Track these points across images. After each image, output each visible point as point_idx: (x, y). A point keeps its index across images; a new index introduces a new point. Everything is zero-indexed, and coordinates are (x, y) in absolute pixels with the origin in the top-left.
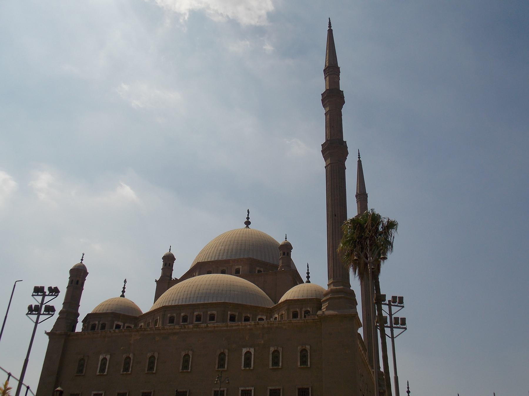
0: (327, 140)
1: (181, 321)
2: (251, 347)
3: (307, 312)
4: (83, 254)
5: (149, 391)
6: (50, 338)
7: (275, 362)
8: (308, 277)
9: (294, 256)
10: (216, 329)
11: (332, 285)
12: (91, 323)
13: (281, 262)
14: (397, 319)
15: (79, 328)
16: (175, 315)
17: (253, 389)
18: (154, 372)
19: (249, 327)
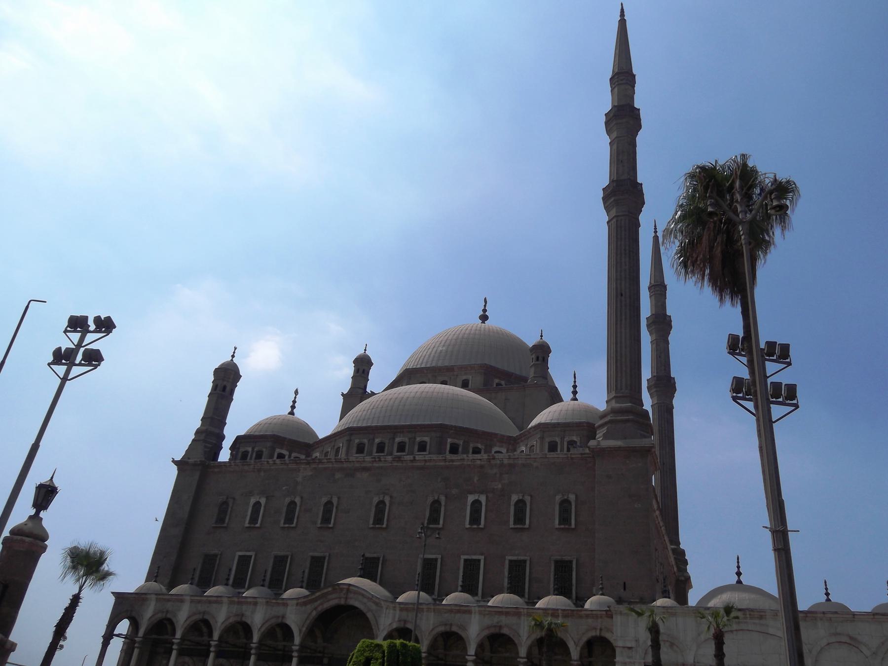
0: (612, 181)
1: (375, 450)
2: (481, 493)
3: (572, 443)
4: (235, 349)
5: (322, 554)
6: (180, 470)
7: (520, 518)
8: (575, 393)
9: (553, 362)
10: (428, 464)
11: (614, 401)
12: (242, 450)
13: (532, 370)
14: (777, 386)
15: (224, 456)
16: (366, 441)
17: (482, 558)
18: (331, 526)
19: (478, 462)
